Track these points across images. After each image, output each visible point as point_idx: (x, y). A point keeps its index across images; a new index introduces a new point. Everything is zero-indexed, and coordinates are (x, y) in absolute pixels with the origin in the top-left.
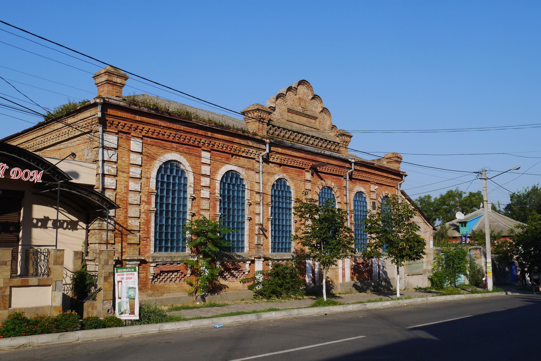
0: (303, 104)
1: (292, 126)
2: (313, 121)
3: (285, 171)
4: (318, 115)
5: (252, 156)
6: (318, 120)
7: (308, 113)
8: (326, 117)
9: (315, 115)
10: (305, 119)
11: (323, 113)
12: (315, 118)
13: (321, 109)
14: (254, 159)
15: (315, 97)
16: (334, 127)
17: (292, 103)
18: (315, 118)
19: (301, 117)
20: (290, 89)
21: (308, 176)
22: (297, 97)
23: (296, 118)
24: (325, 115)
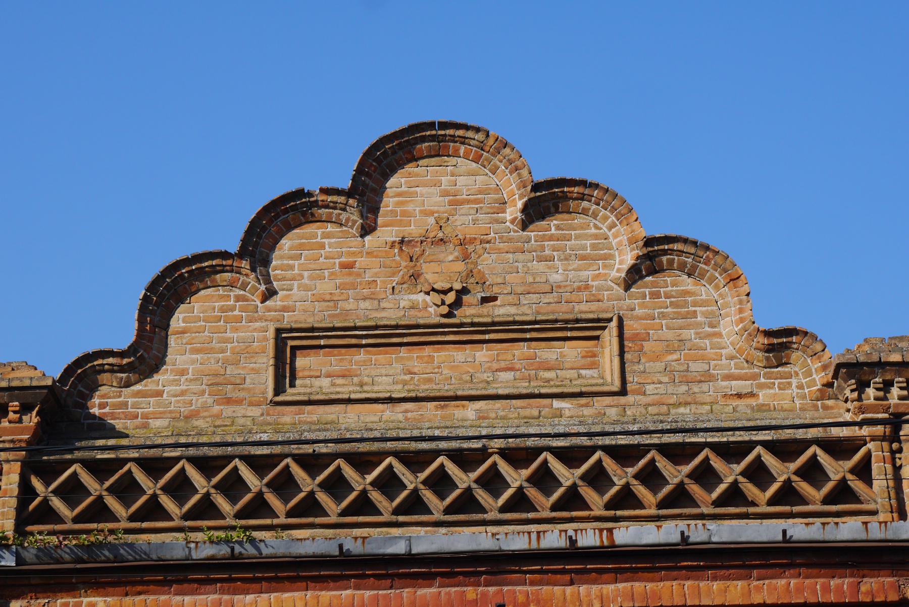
0: (443, 269)
2: (572, 351)
6: (610, 336)
7: (501, 311)
8: (705, 291)
9: (585, 309)
10: (482, 354)
11: (673, 283)
12: (588, 329)
13: (628, 258)
15: (547, 200)
16: (779, 344)
17: (326, 287)
18: (588, 329)
20: (288, 211)
22: (386, 234)
23: (385, 371)
24: (687, 283)
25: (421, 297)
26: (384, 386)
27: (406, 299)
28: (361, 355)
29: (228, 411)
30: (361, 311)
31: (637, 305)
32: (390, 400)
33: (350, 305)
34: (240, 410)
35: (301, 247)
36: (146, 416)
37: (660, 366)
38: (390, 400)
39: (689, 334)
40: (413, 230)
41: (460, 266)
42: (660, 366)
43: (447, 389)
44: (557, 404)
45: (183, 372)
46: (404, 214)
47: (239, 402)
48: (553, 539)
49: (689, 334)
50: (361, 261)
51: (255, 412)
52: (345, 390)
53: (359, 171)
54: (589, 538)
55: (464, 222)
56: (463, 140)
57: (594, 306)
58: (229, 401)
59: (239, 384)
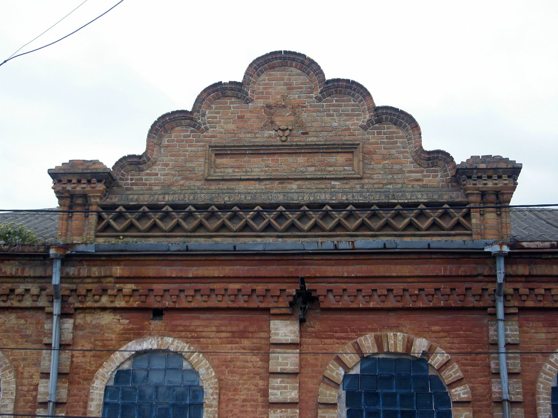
0: (284, 119)
1: (230, 191)
2: (341, 158)
3: (173, 331)
4: (359, 136)
5: (28, 302)
7: (311, 140)
9: (347, 138)
10: (301, 159)
14: (42, 309)
17: (231, 126)
18: (349, 148)
19: (280, 159)
21: (284, 330)
23: (258, 166)
24: (394, 129)
25: (273, 132)
26: (257, 172)
27: (267, 133)
28: (246, 159)
29: (187, 183)
30: (247, 138)
31: (372, 137)
32: (259, 180)
33: (242, 135)
34: (192, 183)
35: (221, 108)
36: (151, 185)
37: (380, 166)
38: (259, 180)
39: (393, 151)
40: (271, 101)
41: (292, 118)
42: (380, 166)
43: (284, 175)
44: (333, 183)
45: (167, 165)
46: (268, 93)
47: (192, 179)
48: (328, 244)
49: (393, 151)
50: (248, 115)
51: (198, 184)
52: (238, 175)
53: (247, 73)
54: (344, 244)
55: (294, 97)
56: (294, 60)
57: (351, 138)
58: (187, 179)
59: (192, 170)
